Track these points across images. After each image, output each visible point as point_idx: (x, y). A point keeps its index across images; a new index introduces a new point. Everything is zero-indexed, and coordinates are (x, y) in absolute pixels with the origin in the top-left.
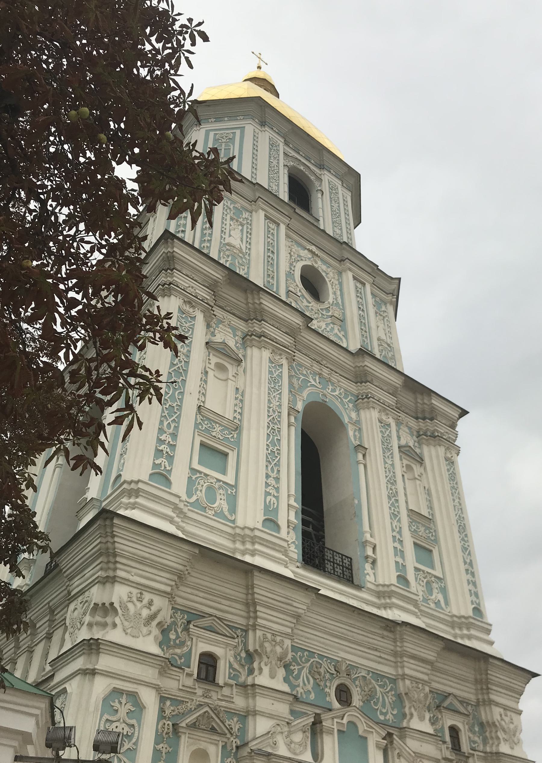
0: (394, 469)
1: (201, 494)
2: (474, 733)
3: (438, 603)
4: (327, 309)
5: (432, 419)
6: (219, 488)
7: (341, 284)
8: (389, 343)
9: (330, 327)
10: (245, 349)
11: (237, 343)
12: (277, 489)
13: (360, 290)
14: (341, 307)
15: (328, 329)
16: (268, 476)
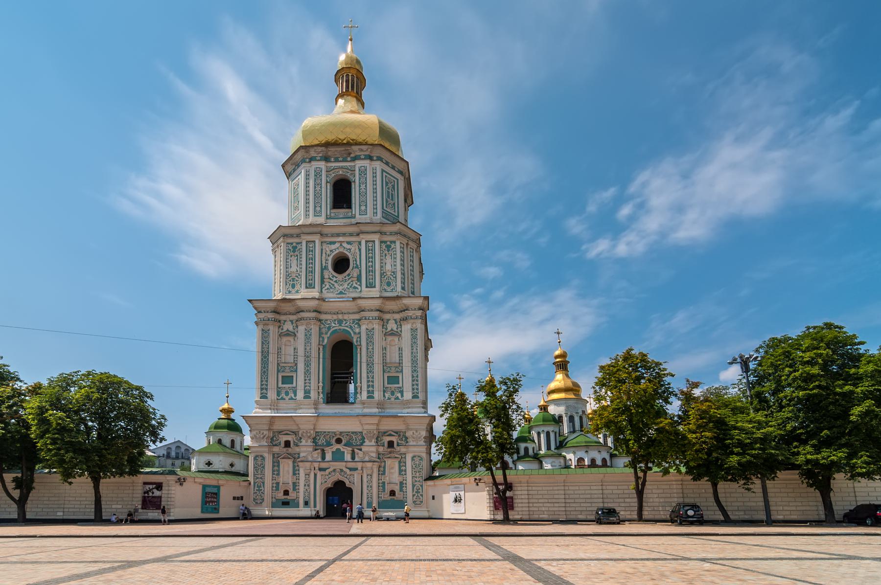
0: (373, 350)
1: (283, 395)
2: (402, 440)
3: (397, 398)
4: (349, 275)
5: (407, 310)
6: (290, 390)
7: (360, 250)
8: (393, 270)
9: (350, 285)
10: (297, 328)
11: (293, 327)
12: (310, 383)
13: (370, 248)
14: (359, 266)
15: (349, 287)
16: (305, 380)
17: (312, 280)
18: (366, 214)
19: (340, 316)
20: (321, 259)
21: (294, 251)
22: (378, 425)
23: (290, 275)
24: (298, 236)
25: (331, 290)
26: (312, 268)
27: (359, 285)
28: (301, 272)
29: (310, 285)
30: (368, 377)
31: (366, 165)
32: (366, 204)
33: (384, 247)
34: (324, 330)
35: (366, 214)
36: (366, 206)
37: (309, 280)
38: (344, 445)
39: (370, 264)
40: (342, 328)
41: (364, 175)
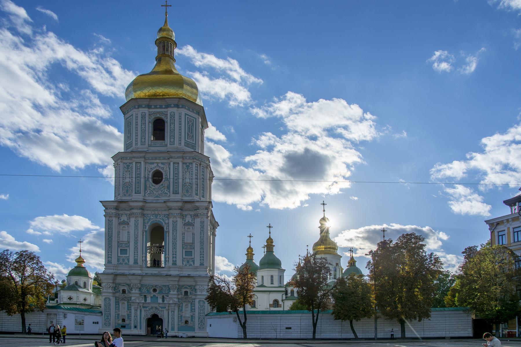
4: (162, 185)
7: (170, 169)
13: (176, 167)
17: (139, 188)
18: (174, 145)
19: (156, 212)
20: (145, 174)
21: (128, 168)
22: (178, 281)
23: (125, 184)
24: (131, 158)
25: (151, 195)
26: (139, 180)
27: (168, 192)
28: (132, 182)
29: (138, 191)
30: (173, 252)
31: (174, 111)
32: (174, 138)
33: (185, 167)
34: (146, 221)
35: (174, 145)
36: (174, 139)
37: (137, 188)
38: (158, 293)
39: (176, 178)
40: (158, 220)
41: (173, 118)
